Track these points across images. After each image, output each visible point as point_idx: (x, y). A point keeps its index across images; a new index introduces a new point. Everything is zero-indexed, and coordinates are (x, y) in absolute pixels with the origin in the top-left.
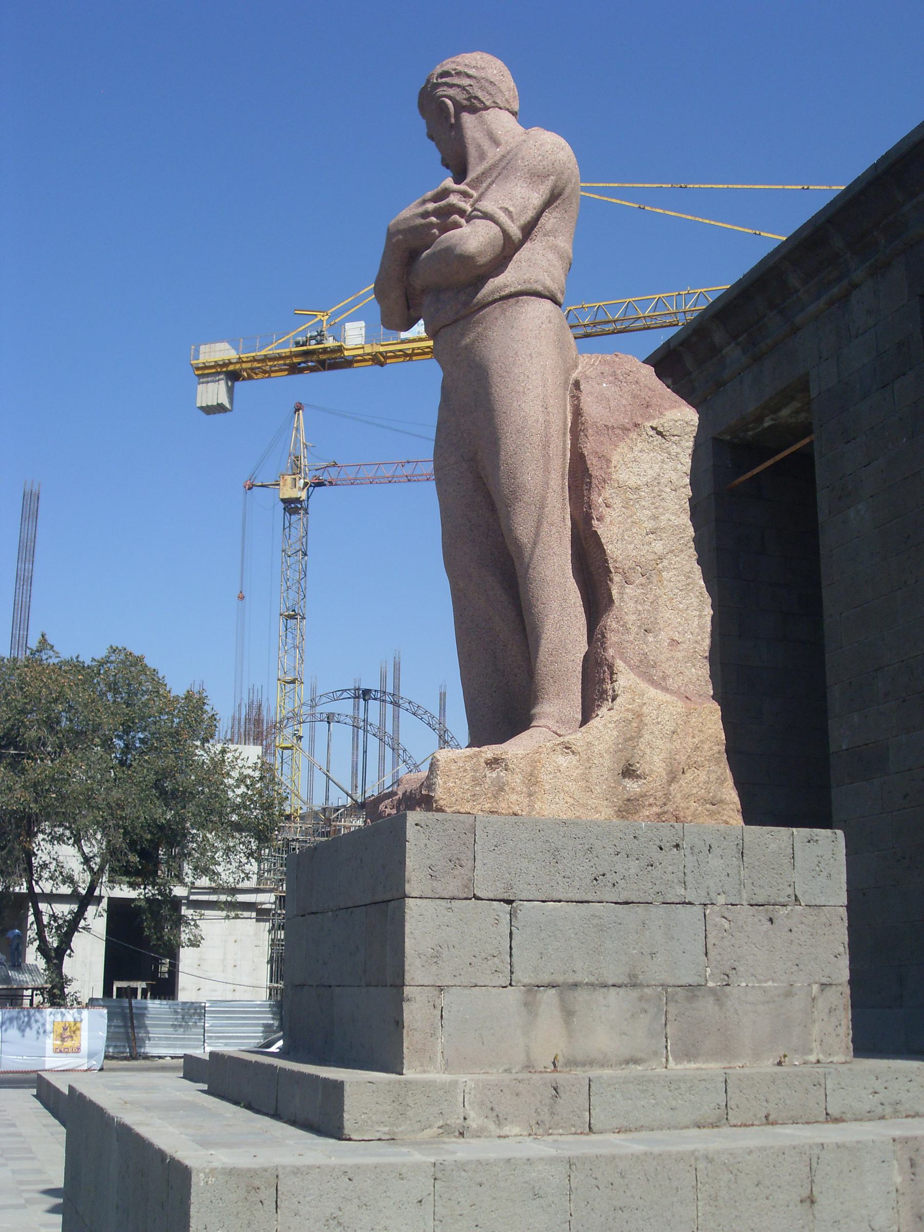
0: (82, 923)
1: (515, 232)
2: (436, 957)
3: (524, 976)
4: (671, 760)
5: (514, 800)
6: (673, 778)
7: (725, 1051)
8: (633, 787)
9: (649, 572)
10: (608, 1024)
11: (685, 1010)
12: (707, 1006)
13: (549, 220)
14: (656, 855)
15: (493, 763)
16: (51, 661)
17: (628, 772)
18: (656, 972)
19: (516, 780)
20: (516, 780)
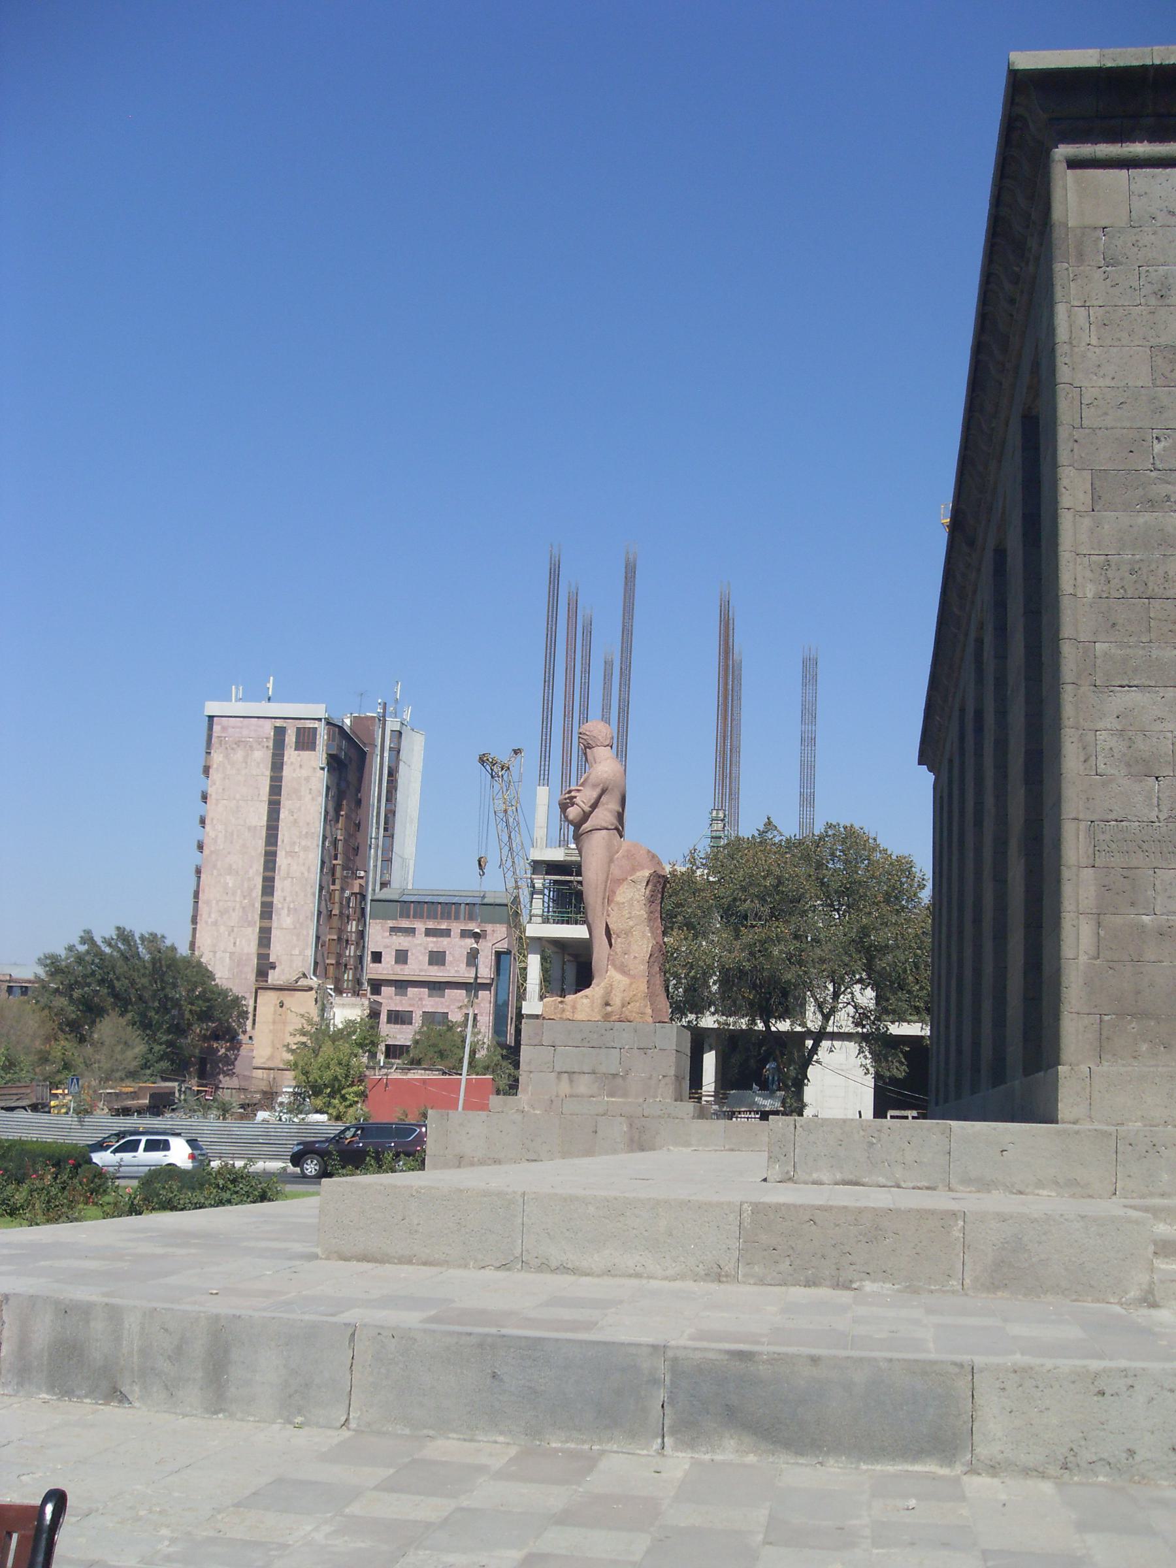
0: (815, 1057)
1: (587, 809)
2: (529, 1063)
3: (558, 1069)
4: (623, 999)
5: (568, 1015)
6: (623, 1006)
7: (625, 1095)
8: (609, 1009)
9: (628, 933)
10: (584, 1085)
11: (612, 1082)
12: (620, 1080)
13: (604, 799)
14: (603, 1032)
15: (561, 1002)
16: (777, 840)
17: (607, 1004)
18: (602, 1069)
19: (568, 1008)
20: (568, 1008)
